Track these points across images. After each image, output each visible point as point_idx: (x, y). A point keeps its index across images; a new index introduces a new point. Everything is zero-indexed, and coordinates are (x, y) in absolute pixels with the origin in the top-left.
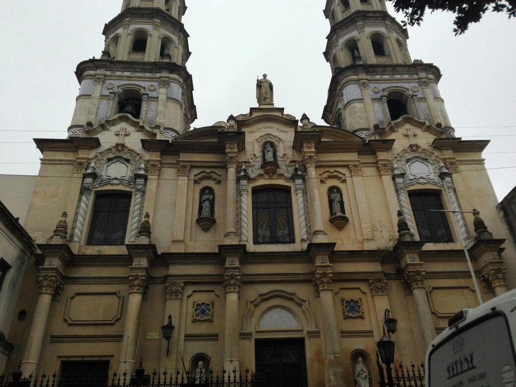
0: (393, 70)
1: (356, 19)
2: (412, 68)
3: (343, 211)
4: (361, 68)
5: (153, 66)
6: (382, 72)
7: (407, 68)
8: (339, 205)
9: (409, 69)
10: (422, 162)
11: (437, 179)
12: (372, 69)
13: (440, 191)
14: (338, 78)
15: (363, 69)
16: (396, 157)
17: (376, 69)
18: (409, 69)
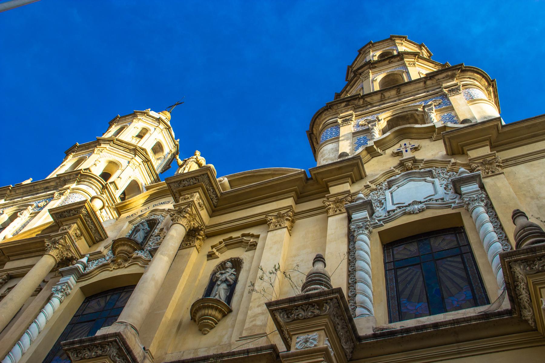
0: (398, 92)
1: (360, 71)
2: (429, 82)
3: (229, 298)
4: (343, 104)
5: (58, 181)
6: (380, 101)
7: (422, 84)
8: (224, 286)
9: (425, 83)
10: (420, 181)
11: (450, 196)
12: (361, 101)
13: (458, 216)
14: (315, 132)
15: (346, 106)
16: (367, 187)
17: (368, 99)
18: (425, 83)
